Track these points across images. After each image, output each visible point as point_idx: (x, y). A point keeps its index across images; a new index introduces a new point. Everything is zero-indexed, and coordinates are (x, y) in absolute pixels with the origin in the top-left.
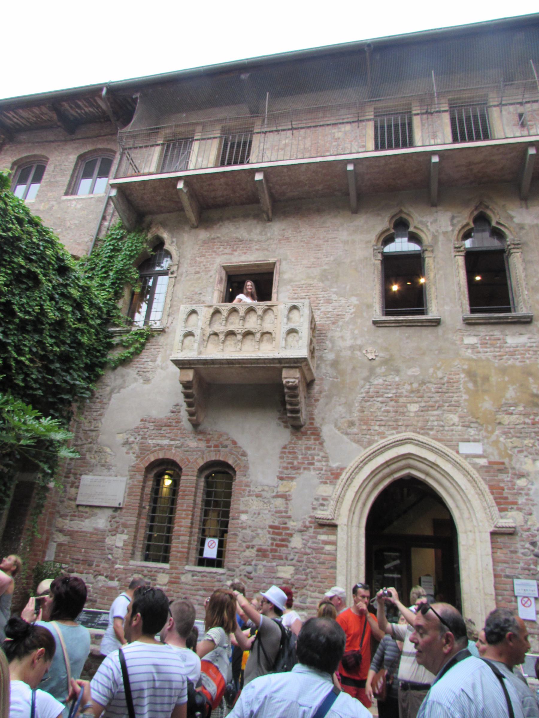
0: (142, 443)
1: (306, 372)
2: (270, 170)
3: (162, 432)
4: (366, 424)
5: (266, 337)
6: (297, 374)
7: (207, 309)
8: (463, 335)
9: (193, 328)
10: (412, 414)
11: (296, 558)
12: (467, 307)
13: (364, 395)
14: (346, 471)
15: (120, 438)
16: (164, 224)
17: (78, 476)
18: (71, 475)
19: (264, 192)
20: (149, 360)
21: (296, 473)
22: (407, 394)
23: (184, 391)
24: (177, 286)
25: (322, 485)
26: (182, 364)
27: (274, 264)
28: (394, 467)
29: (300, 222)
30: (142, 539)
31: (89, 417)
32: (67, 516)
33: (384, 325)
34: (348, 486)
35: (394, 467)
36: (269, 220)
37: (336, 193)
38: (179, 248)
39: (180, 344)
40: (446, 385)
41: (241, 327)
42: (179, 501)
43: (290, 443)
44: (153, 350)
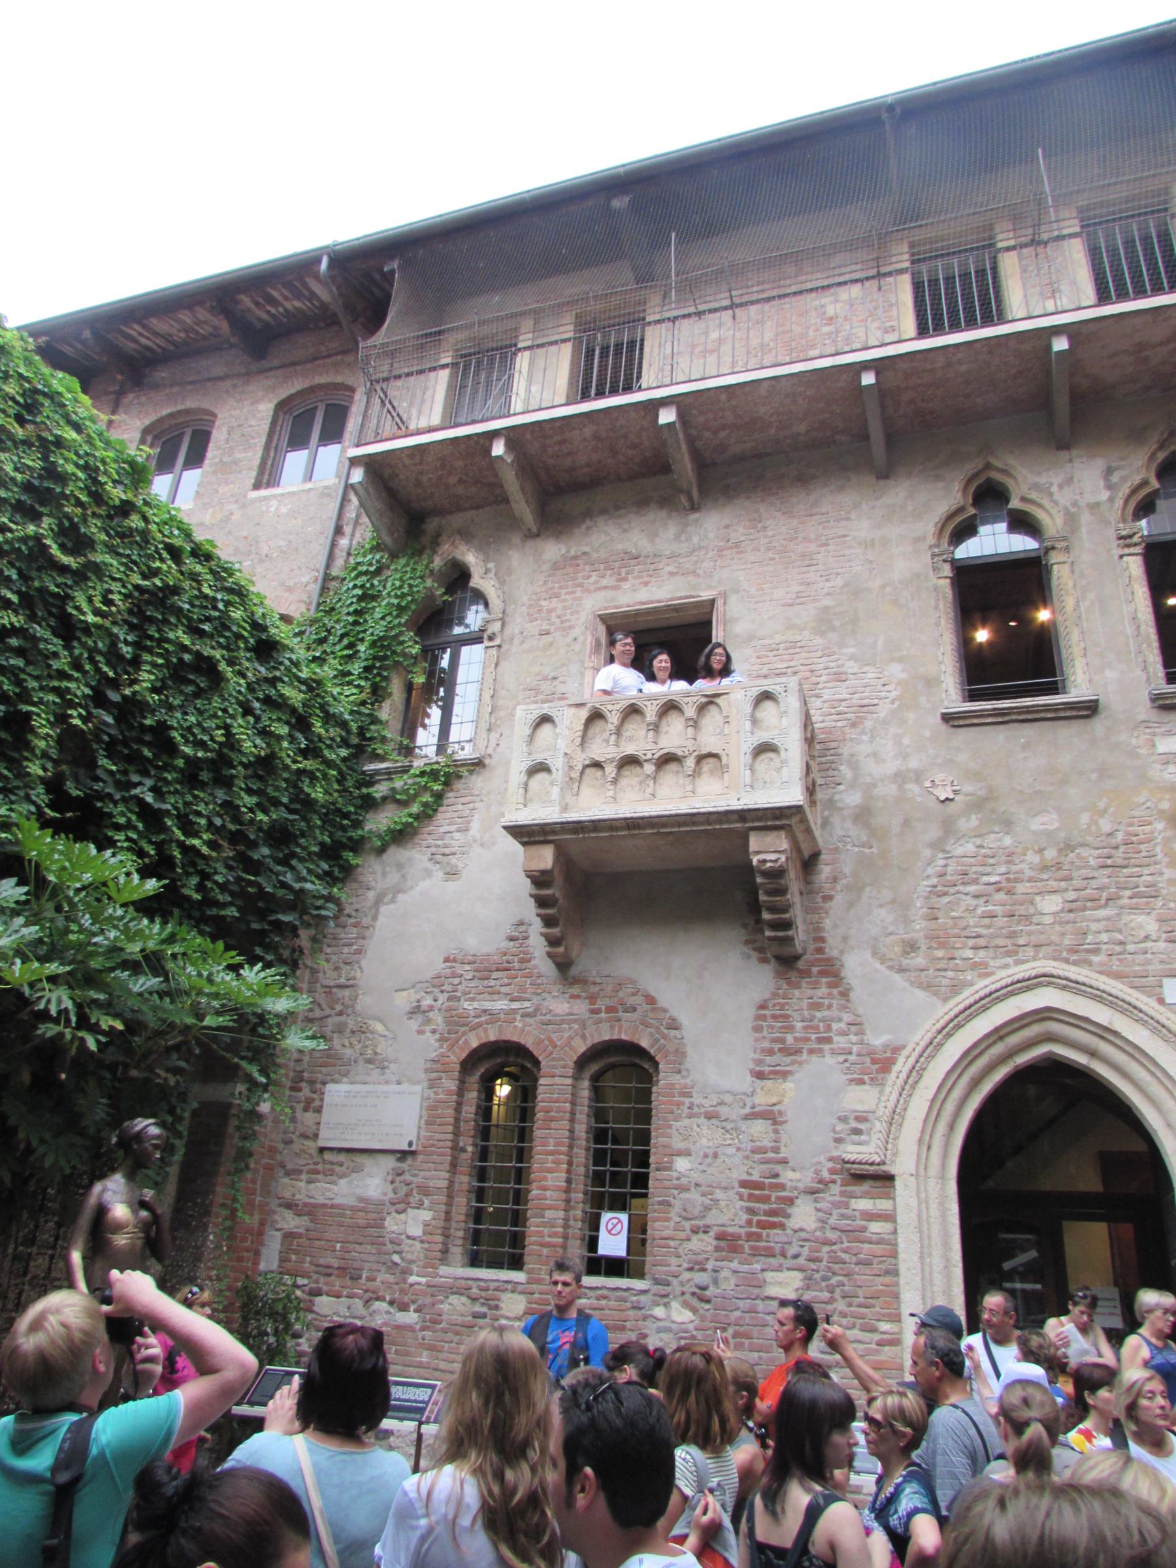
0: (449, 1009)
1: (801, 837)
2: (689, 400)
3: (492, 983)
4: (942, 946)
5: (707, 765)
6: (781, 842)
7: (573, 711)
8: (1154, 734)
9: (546, 754)
10: (1047, 920)
11: (805, 1252)
12: (1160, 672)
13: (934, 881)
14: (905, 1053)
15: (403, 1000)
16: (466, 535)
17: (319, 1086)
18: (304, 1085)
19: (680, 448)
20: (453, 828)
21: (793, 1063)
22: (1033, 874)
23: (535, 892)
24: (504, 665)
25: (853, 1087)
26: (527, 835)
27: (712, 602)
28: (1014, 1039)
29: (762, 508)
30: (463, 1218)
31: (334, 958)
32: (301, 1172)
33: (968, 722)
34: (913, 1087)
35: (1014, 1039)
36: (694, 508)
37: (838, 437)
38: (502, 583)
39: (522, 791)
40: (1122, 849)
41: (651, 746)
42: (538, 1133)
43: (775, 995)
44: (460, 807)
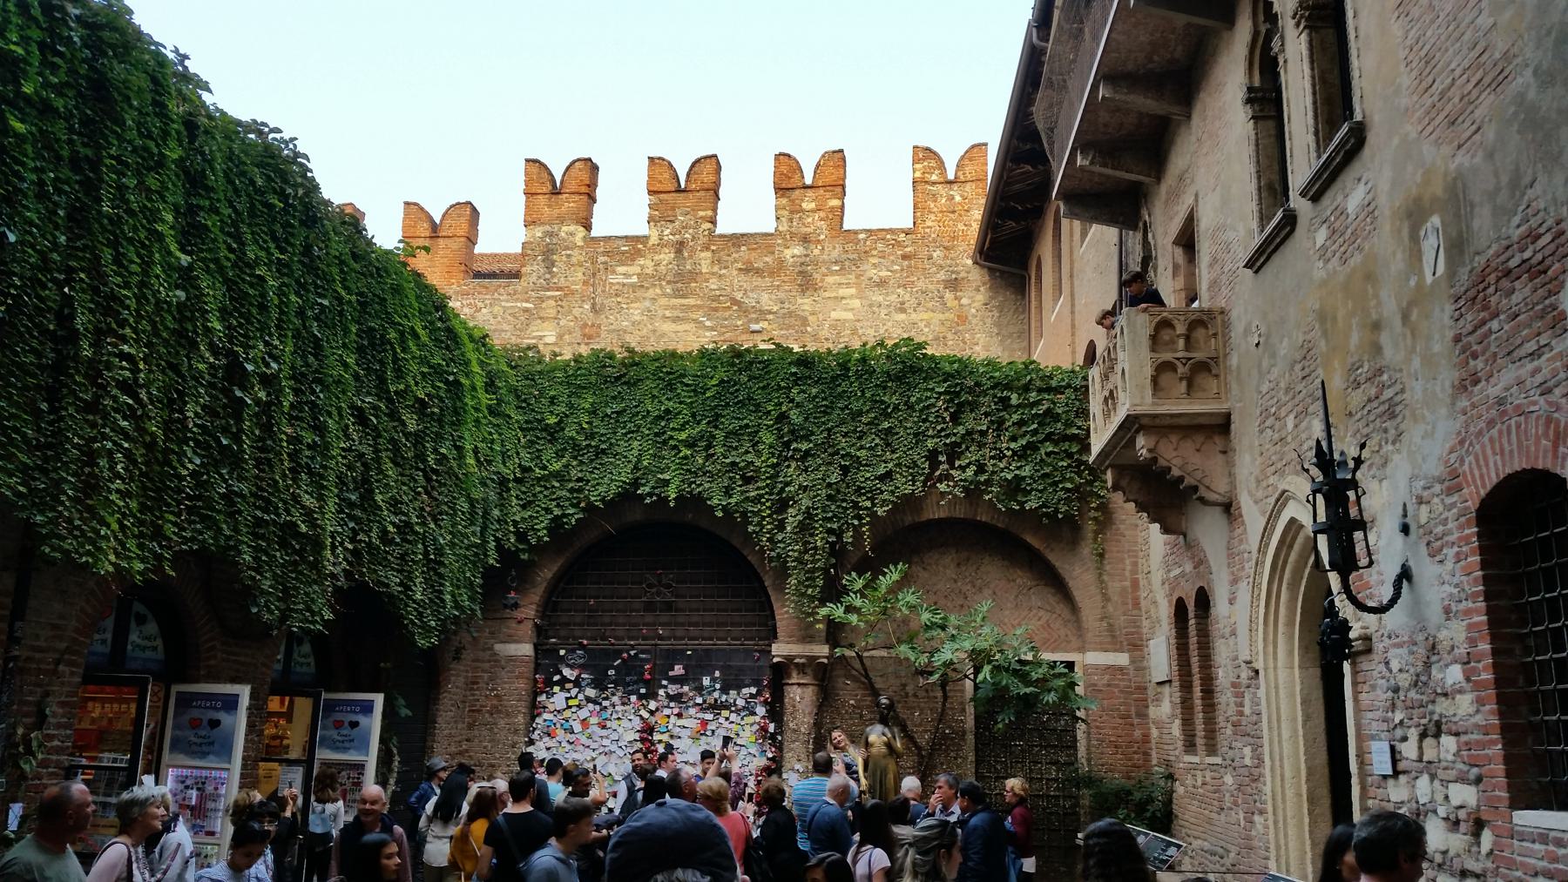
36: (1189, 117)
